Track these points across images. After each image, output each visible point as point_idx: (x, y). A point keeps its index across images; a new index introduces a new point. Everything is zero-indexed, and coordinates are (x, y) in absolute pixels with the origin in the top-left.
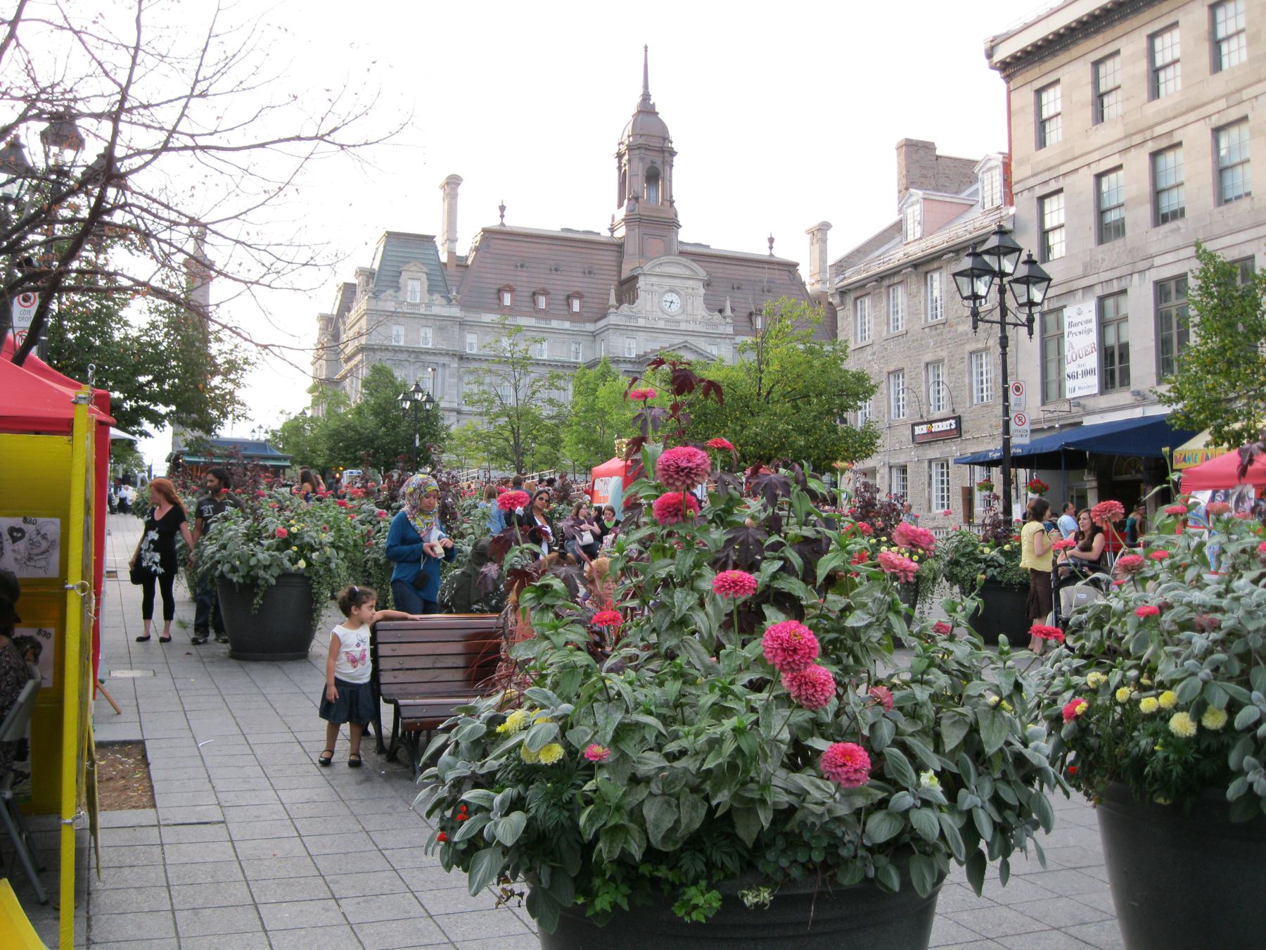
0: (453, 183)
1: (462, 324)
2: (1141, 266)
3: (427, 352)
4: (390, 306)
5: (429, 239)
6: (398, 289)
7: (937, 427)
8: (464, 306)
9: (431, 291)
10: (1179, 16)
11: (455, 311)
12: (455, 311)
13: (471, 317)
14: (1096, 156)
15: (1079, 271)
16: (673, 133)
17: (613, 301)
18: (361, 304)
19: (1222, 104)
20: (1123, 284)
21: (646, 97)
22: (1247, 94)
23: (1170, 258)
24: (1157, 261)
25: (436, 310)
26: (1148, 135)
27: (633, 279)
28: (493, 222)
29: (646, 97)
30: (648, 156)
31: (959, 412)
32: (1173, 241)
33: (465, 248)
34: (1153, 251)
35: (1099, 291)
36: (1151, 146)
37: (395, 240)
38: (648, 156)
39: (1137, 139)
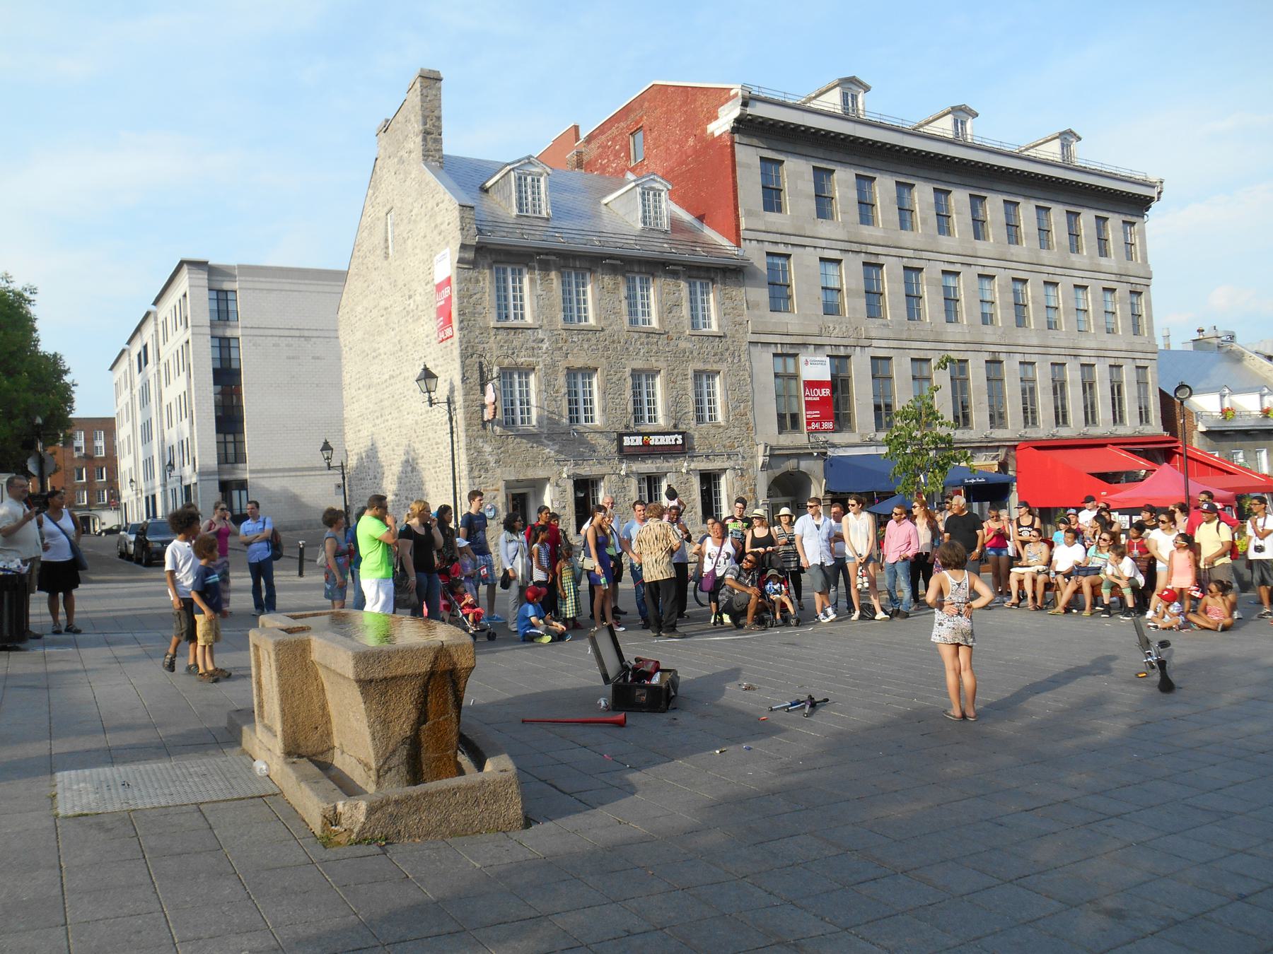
2: (866, 342)
7: (654, 441)
10: (877, 176)
14: (823, 243)
15: (816, 331)
19: (910, 253)
20: (849, 351)
22: (925, 255)
23: (883, 343)
24: (875, 343)
26: (864, 248)
31: (682, 427)
32: (886, 333)
34: (873, 334)
35: (828, 350)
36: (863, 257)
39: (855, 247)
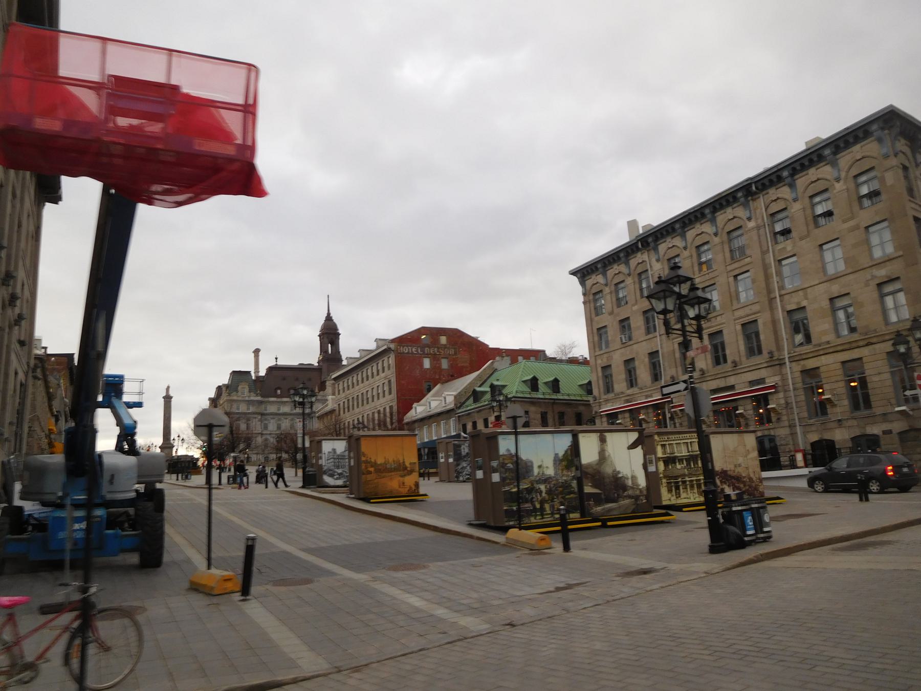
0: (257, 352)
1: (261, 402)
3: (249, 413)
4: (235, 398)
5: (249, 372)
6: (237, 391)
8: (262, 397)
9: (250, 392)
11: (259, 398)
12: (259, 398)
13: (266, 399)
16: (339, 327)
17: (317, 390)
18: (224, 397)
21: (329, 314)
25: (252, 398)
27: (325, 382)
28: (273, 363)
29: (329, 314)
30: (330, 334)
33: (262, 373)
37: (235, 373)
38: (330, 334)
